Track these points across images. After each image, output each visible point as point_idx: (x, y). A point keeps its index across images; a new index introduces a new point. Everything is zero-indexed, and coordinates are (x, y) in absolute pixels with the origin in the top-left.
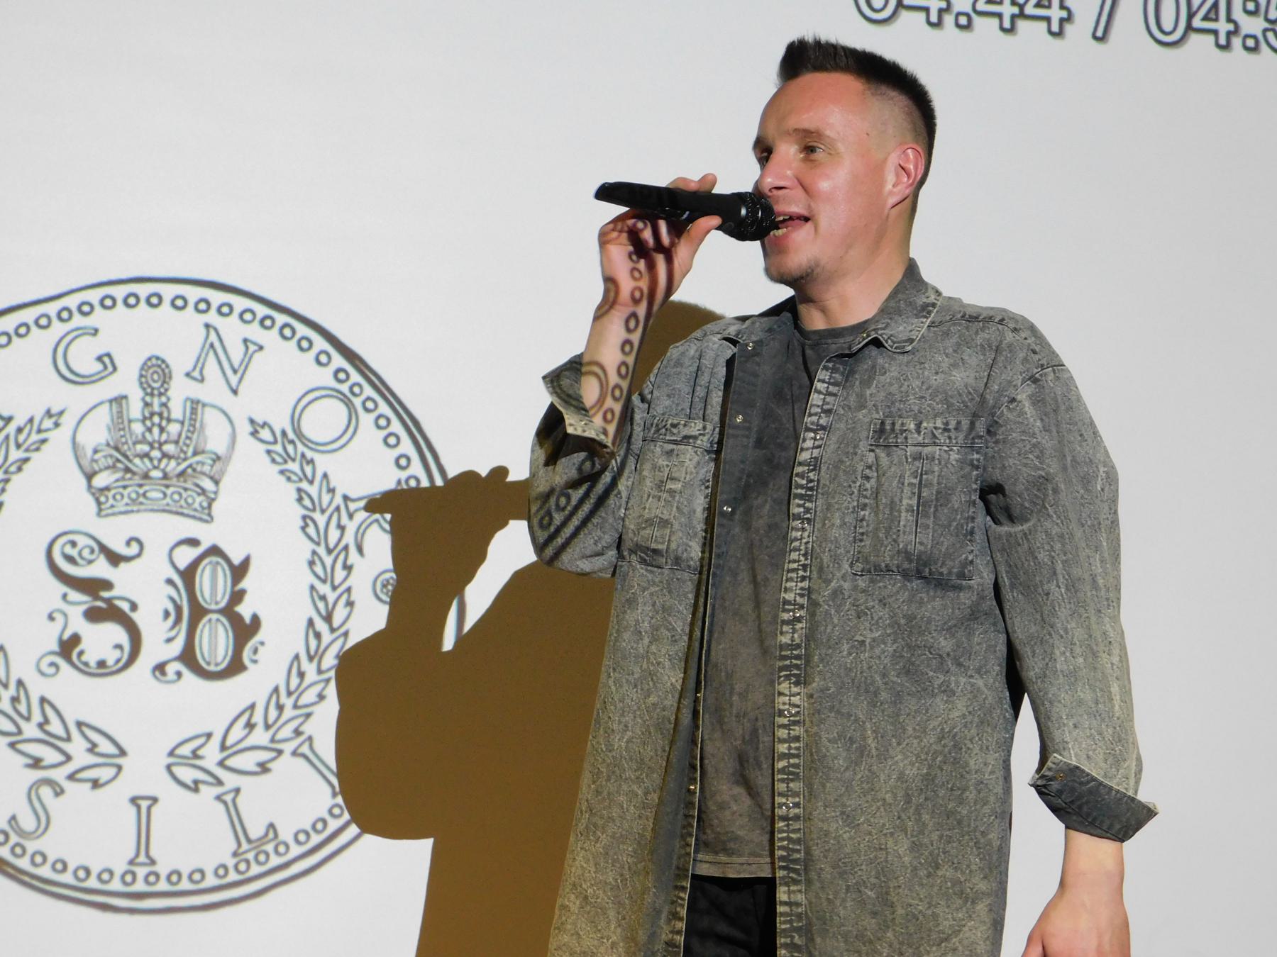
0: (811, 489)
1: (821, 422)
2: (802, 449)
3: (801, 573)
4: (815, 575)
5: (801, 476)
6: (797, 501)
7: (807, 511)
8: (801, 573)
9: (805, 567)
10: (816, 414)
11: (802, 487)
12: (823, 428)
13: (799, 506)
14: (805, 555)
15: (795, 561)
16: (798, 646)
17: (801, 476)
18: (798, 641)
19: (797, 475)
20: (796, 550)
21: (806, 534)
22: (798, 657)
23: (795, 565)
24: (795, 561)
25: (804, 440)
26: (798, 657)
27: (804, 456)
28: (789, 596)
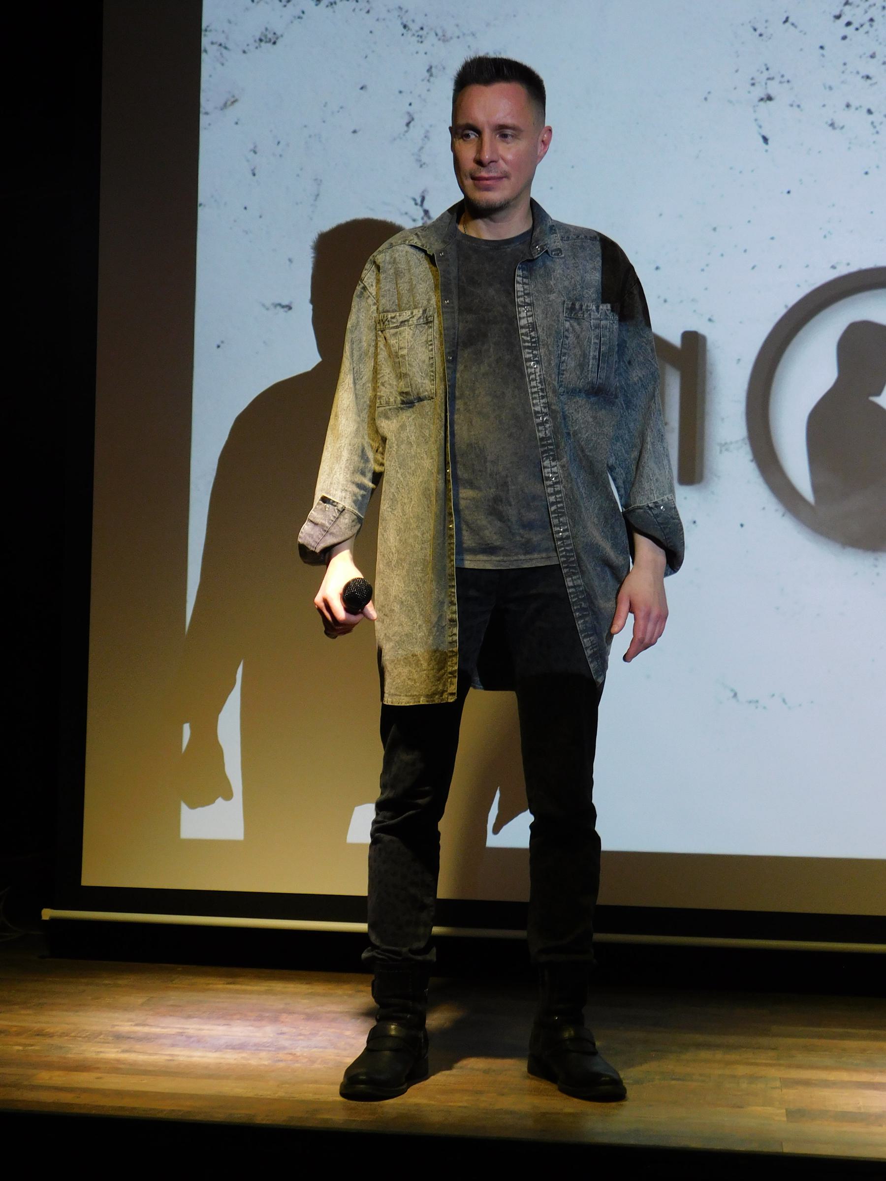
0: (534, 342)
1: (527, 300)
2: (520, 318)
3: (541, 394)
4: (550, 394)
5: (526, 334)
6: (527, 350)
7: (535, 356)
8: (541, 394)
9: (542, 390)
10: (521, 296)
11: (528, 341)
12: (528, 304)
13: (529, 353)
14: (540, 382)
15: (534, 387)
16: (549, 438)
17: (526, 334)
18: (549, 435)
19: (522, 334)
20: (533, 380)
21: (538, 370)
22: (551, 444)
23: (536, 390)
24: (534, 387)
25: (520, 313)
26: (551, 444)
27: (523, 322)
28: (538, 409)
